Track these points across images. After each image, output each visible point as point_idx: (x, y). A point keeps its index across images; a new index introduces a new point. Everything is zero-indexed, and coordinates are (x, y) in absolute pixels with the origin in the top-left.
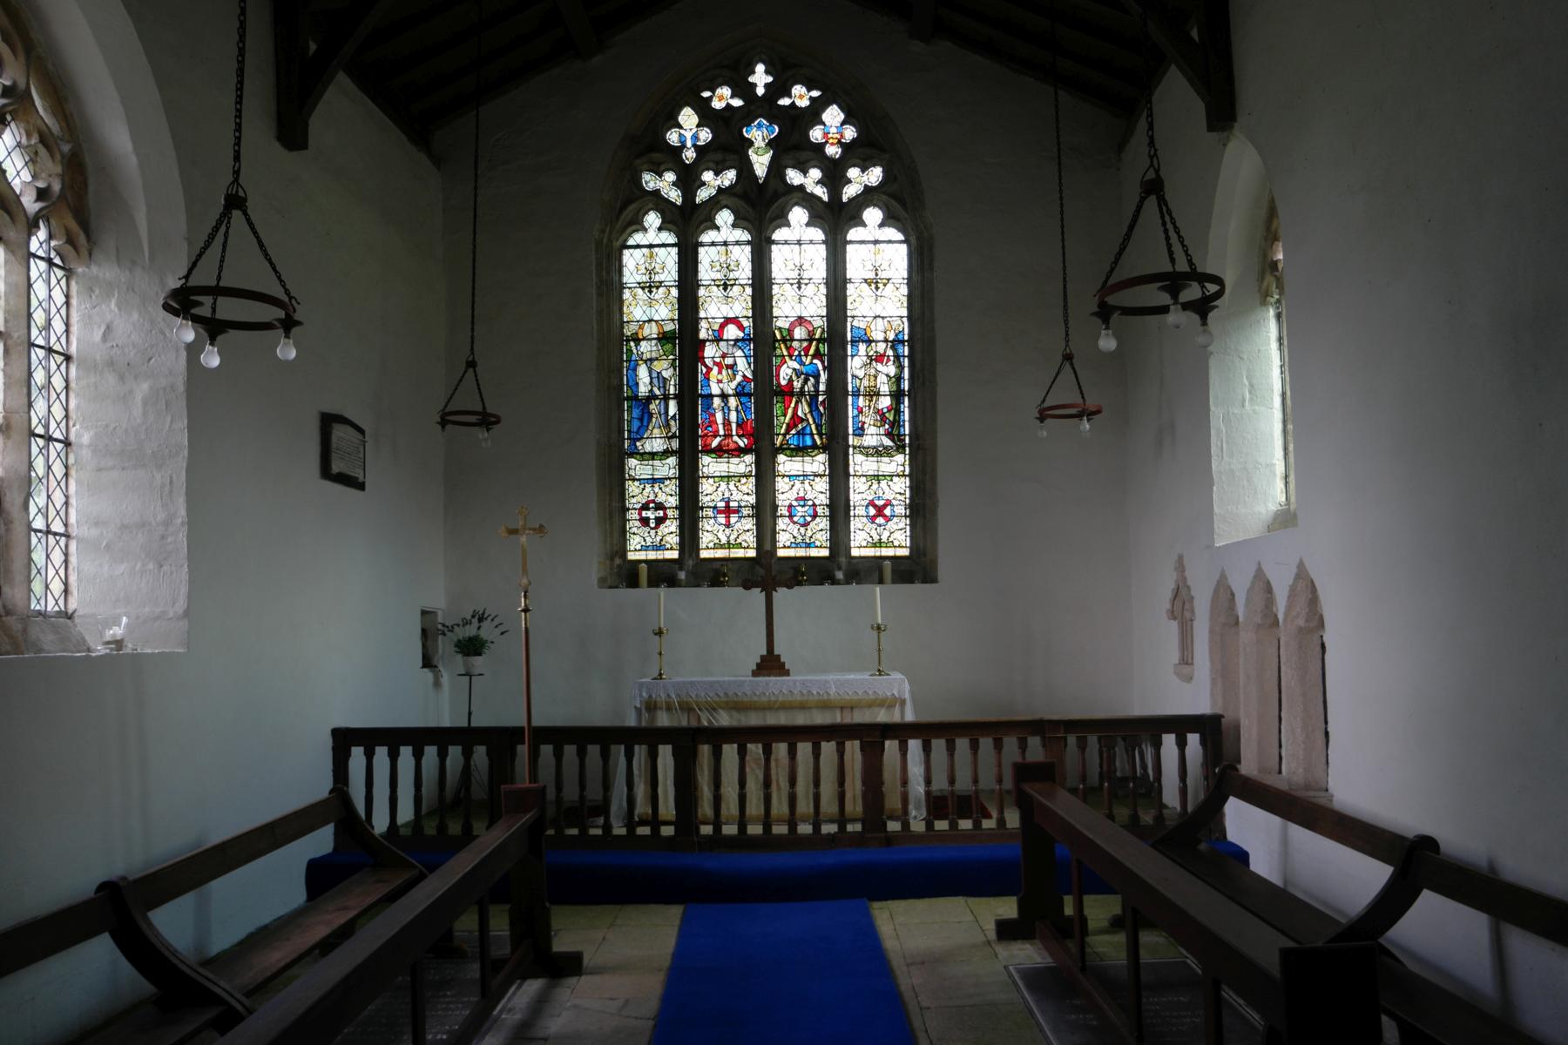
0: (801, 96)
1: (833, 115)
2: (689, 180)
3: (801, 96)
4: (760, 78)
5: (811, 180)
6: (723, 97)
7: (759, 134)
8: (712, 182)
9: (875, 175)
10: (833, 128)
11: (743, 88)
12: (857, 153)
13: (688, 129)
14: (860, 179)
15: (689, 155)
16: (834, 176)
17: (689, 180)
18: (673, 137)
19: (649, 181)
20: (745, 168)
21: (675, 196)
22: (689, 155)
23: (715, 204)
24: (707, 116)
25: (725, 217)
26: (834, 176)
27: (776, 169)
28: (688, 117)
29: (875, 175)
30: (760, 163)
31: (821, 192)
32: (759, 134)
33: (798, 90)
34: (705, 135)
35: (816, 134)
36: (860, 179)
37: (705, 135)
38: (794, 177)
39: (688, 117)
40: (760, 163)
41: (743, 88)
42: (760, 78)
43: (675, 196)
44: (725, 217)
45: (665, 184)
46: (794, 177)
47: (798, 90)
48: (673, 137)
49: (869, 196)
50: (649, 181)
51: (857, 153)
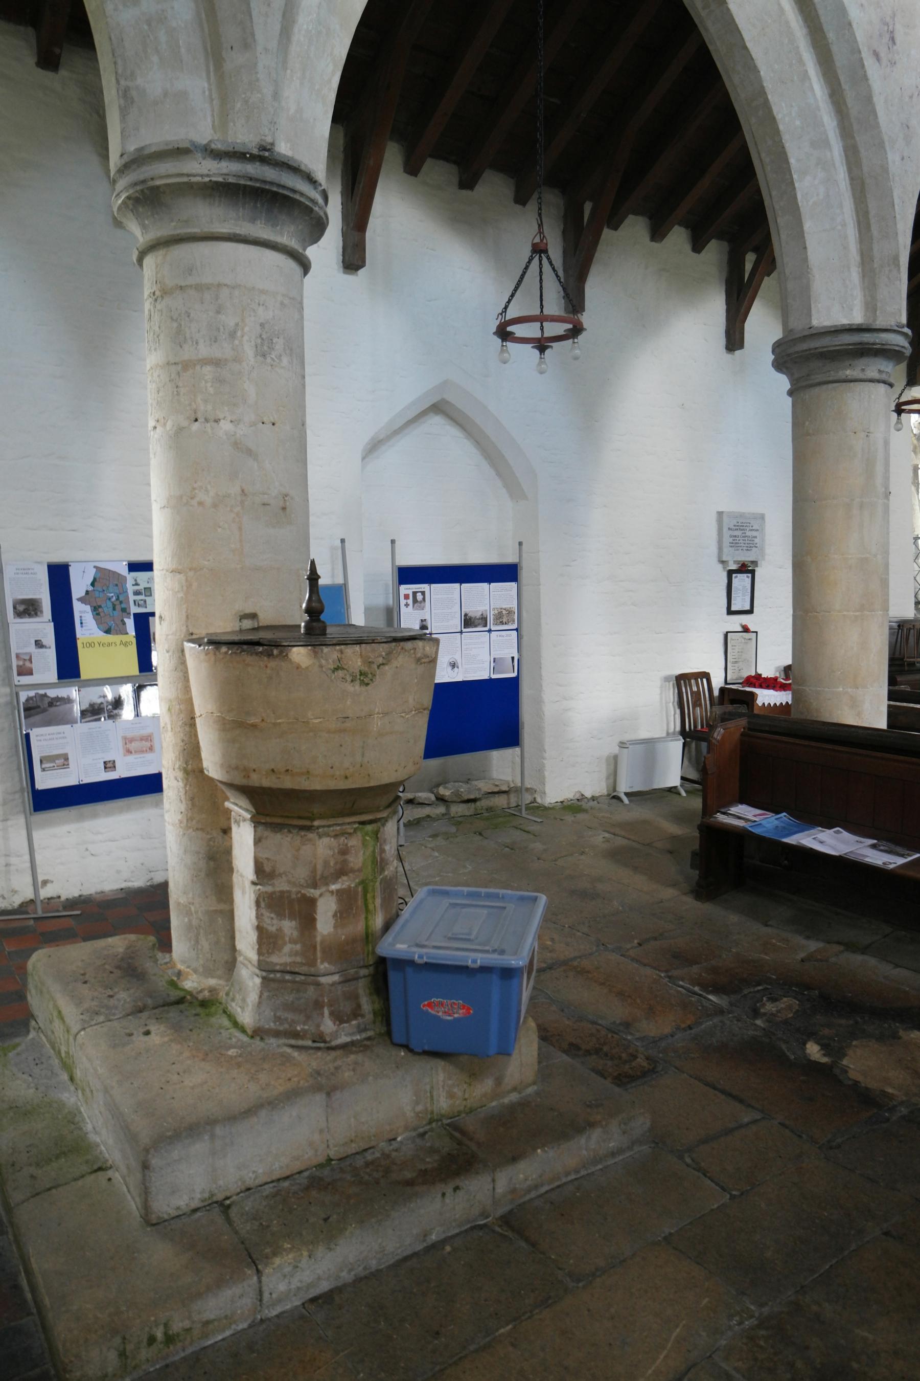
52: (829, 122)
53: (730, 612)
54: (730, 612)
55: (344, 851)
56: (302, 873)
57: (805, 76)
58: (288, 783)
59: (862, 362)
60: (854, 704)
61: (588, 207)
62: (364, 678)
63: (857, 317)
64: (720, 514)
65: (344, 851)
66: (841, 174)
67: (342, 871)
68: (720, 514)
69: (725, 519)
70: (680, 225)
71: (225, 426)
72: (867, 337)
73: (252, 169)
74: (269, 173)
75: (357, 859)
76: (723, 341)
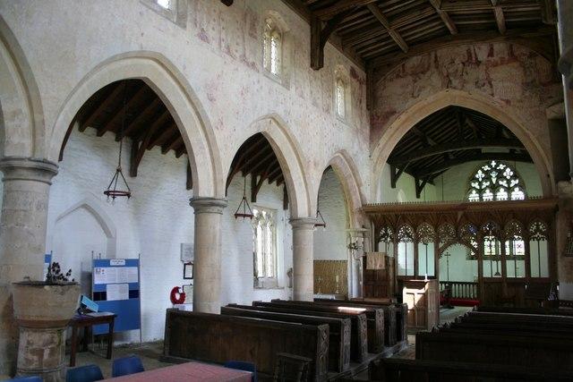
0: (502, 167)
1: (508, 170)
2: (480, 184)
3: (502, 167)
4: (494, 164)
5: (504, 183)
6: (486, 168)
7: (494, 175)
8: (485, 184)
9: (517, 181)
10: (508, 173)
11: (490, 166)
12: (514, 177)
13: (480, 175)
14: (514, 182)
15: (480, 180)
16: (509, 182)
17: (480, 184)
18: (477, 176)
19: (473, 185)
20: (491, 182)
21: (478, 187)
22: (480, 180)
23: (485, 189)
24: (483, 172)
25: (488, 191)
26: (509, 182)
27: (497, 182)
28: (480, 172)
29: (517, 181)
30: (494, 180)
31: (506, 185)
32: (494, 175)
33: (501, 165)
34: (483, 176)
35: (505, 174)
36: (514, 182)
37: (483, 176)
38: (501, 183)
39: (480, 172)
40: (494, 180)
41: (490, 166)
42: (494, 164)
43: (478, 187)
44: (488, 191)
45: (476, 185)
46: (501, 183)
47: (501, 165)
48: (477, 176)
49: (516, 185)
50: (473, 185)
51: (514, 177)
52: (205, 143)
53: (184, 278)
54: (184, 278)
55: (53, 337)
56: (41, 343)
57: (198, 131)
58: (41, 319)
59: (213, 207)
60: (210, 308)
61: (140, 143)
62: (62, 293)
63: (212, 195)
64: (182, 244)
65: (53, 337)
66: (208, 156)
67: (52, 342)
68: (182, 244)
69: (184, 247)
70: (174, 149)
71: (26, 227)
72: (214, 201)
73: (40, 164)
74: (45, 165)
75: (56, 340)
76: (185, 187)
